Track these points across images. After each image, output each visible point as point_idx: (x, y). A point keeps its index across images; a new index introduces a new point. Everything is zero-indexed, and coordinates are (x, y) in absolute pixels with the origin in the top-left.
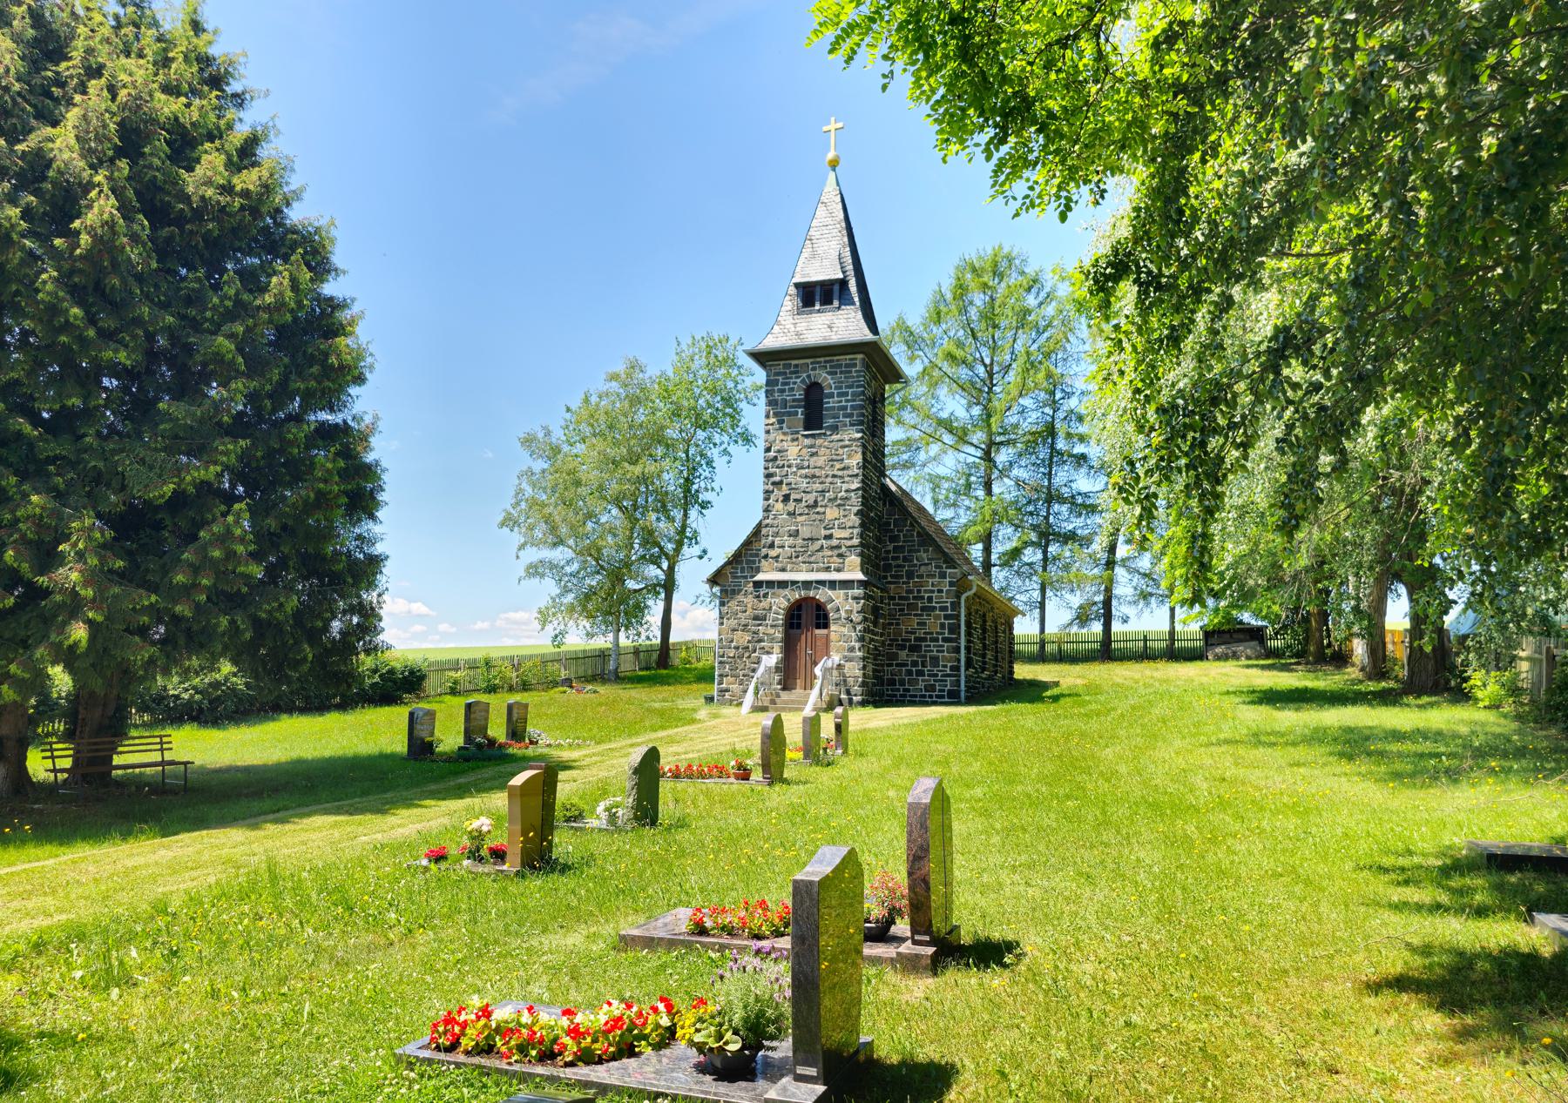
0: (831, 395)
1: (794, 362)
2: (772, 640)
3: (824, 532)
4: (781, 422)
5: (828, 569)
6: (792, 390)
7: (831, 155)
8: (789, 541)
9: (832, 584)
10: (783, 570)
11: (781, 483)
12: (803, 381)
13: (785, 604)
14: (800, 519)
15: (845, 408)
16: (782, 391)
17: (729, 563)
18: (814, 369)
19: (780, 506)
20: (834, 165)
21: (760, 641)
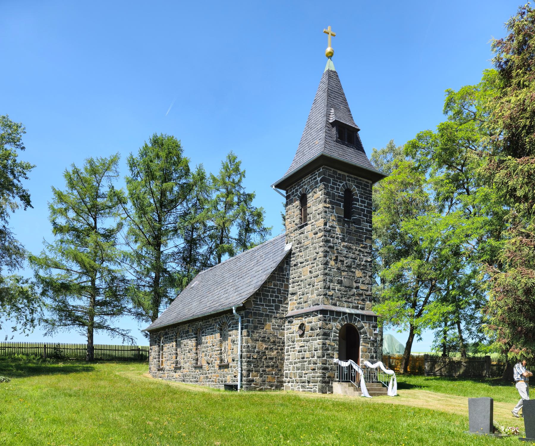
0: (357, 200)
1: (339, 172)
2: (334, 349)
3: (355, 285)
4: (333, 208)
5: (357, 308)
6: (338, 189)
7: (329, 49)
8: (338, 287)
9: (363, 317)
10: (335, 305)
11: (333, 248)
12: (343, 186)
13: (340, 327)
14: (344, 274)
15: (363, 210)
16: (333, 188)
17: (256, 295)
18: (349, 180)
19: (332, 263)
20: (330, 56)
21: (328, 350)
